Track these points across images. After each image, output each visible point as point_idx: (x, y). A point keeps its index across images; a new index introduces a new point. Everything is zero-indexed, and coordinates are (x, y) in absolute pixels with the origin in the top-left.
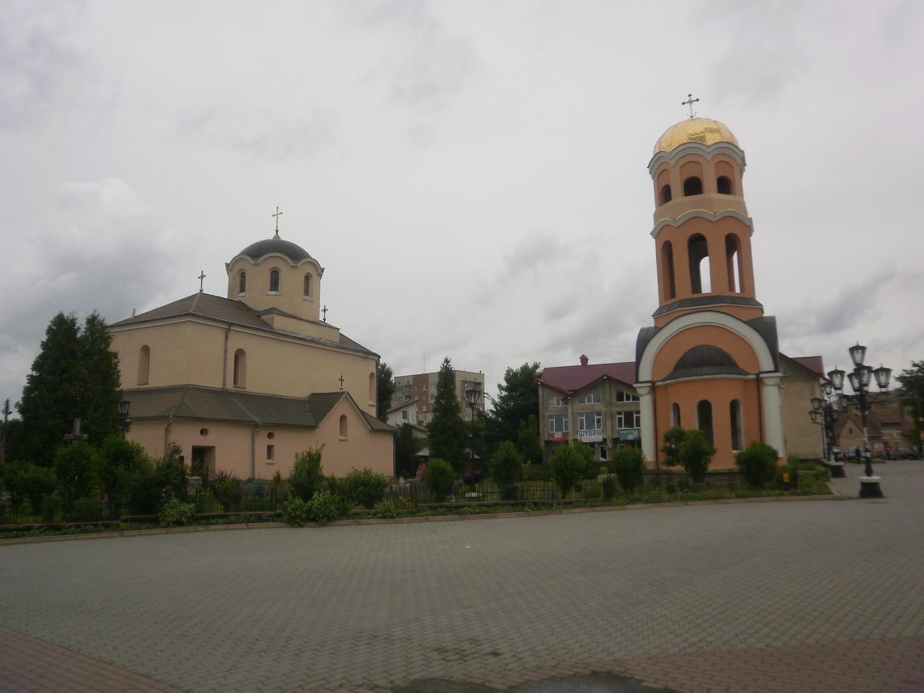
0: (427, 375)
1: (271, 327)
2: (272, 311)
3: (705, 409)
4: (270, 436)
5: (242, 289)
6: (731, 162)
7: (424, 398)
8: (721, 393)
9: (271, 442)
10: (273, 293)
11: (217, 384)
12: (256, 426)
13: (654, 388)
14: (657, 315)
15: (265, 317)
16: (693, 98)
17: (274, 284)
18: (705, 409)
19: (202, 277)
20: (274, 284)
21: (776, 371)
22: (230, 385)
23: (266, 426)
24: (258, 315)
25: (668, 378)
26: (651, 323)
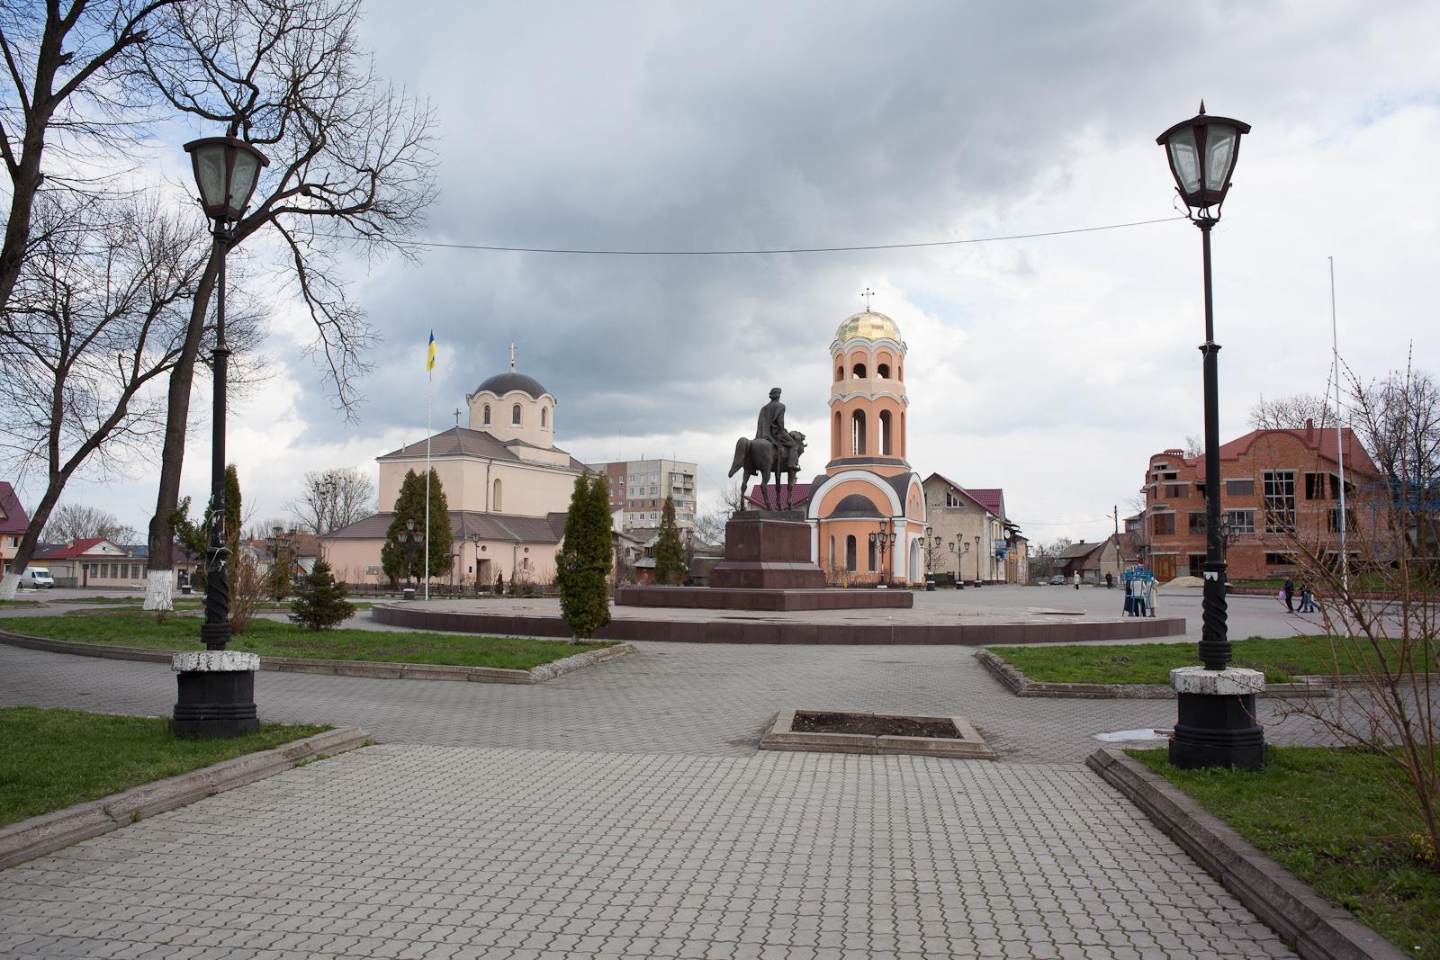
0: (626, 463)
1: (518, 458)
2: (516, 442)
3: (851, 541)
4: (526, 550)
5: (487, 421)
6: (892, 354)
7: (621, 491)
8: (863, 529)
9: (526, 555)
10: (516, 425)
11: (482, 509)
12: (518, 543)
13: (819, 523)
14: (829, 466)
15: (512, 448)
16: (870, 291)
17: (517, 418)
18: (851, 541)
19: (458, 413)
20: (517, 418)
21: (903, 516)
22: (491, 510)
23: (526, 542)
24: (504, 445)
25: (828, 518)
26: (824, 472)
